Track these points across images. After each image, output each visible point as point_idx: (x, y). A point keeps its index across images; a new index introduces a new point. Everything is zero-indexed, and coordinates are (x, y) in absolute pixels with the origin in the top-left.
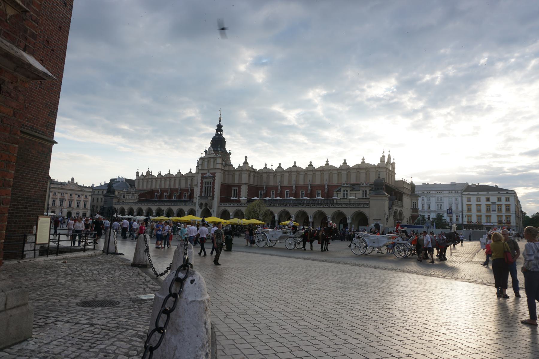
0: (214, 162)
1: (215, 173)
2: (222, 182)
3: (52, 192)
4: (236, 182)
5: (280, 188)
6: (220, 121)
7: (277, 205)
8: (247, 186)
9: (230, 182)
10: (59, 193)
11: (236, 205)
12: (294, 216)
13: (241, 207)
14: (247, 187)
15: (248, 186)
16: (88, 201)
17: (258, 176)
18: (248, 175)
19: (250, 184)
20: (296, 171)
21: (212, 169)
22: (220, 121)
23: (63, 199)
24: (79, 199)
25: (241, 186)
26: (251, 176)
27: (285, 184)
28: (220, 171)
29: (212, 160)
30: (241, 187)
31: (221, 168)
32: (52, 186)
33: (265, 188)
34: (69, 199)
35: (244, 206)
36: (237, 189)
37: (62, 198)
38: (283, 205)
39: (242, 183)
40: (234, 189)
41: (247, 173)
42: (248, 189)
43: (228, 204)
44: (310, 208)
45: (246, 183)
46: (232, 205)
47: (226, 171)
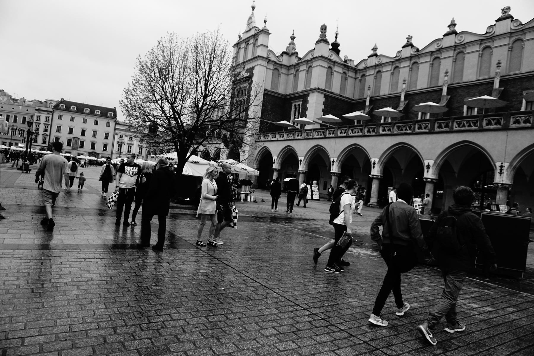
0: (254, 45)
1: (253, 68)
2: (269, 88)
3: (117, 134)
4: (301, 88)
5: (405, 99)
6: (336, 37)
7: (381, 129)
8: (323, 96)
9: (290, 91)
10: (126, 136)
11: (285, 136)
12: (431, 162)
13: (294, 142)
14: (323, 100)
15: (325, 96)
16: (133, 144)
17: (355, 79)
18: (326, 70)
19: (332, 93)
20: (456, 46)
21: (250, 60)
22: (336, 37)
23: (122, 143)
24: (130, 142)
25: (308, 95)
26: (335, 73)
27: (418, 88)
28: (265, 63)
29: (252, 41)
30: (309, 99)
31: (265, 56)
32: (117, 127)
33: (368, 103)
34: (139, 145)
35: (300, 137)
36: (301, 103)
37: (120, 141)
38: (398, 128)
39: (311, 90)
40: (295, 105)
41: (326, 65)
42: (324, 103)
43: (271, 136)
44: (501, 136)
45: (319, 89)
46: (278, 137)
47: (281, 65)
